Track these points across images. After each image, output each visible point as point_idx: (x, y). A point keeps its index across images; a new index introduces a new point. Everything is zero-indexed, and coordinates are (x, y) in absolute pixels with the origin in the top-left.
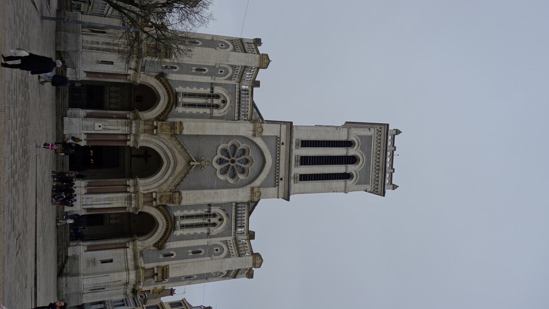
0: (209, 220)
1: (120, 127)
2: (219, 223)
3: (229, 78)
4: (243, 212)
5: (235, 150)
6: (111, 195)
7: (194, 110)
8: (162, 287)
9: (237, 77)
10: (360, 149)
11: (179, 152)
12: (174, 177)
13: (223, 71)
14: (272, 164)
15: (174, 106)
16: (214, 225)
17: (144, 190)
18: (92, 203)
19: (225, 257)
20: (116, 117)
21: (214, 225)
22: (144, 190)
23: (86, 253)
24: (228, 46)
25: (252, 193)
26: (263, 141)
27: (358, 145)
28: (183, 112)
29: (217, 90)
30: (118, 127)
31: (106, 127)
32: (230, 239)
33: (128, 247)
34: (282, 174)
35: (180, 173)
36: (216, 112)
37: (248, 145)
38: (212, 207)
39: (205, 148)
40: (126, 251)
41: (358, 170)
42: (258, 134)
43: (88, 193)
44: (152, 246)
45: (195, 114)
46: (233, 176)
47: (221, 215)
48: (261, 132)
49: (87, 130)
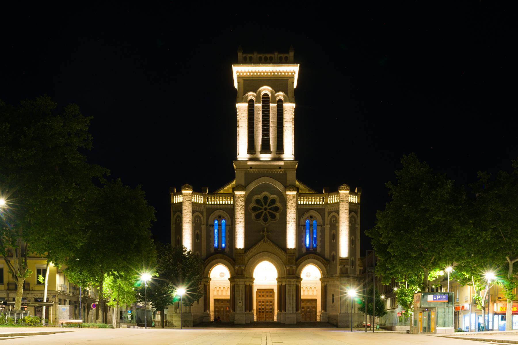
3: (201, 214)
6: (287, 295)
13: (197, 219)
18: (292, 307)
20: (234, 292)
22: (285, 274)
28: (228, 247)
30: (240, 291)
31: (240, 299)
38: (301, 224)
43: (285, 310)
49: (243, 310)
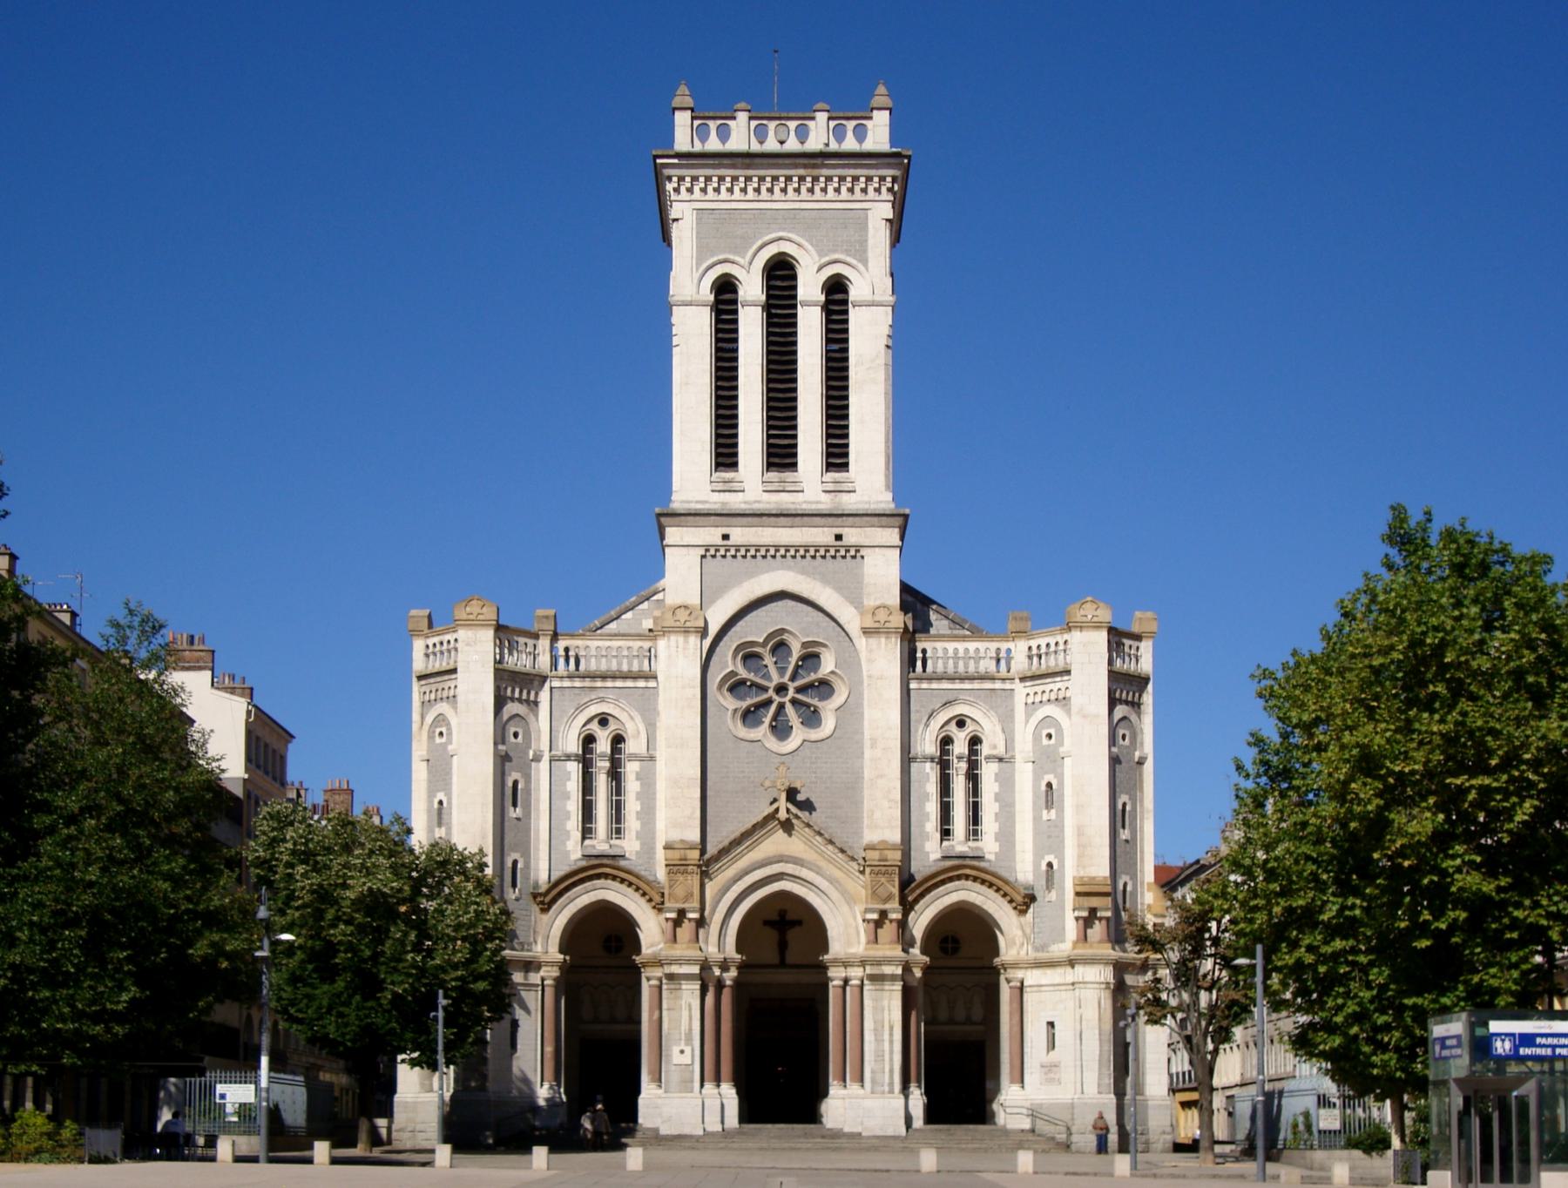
0: (960, 758)
1: (683, 1002)
2: (970, 727)
4: (940, 654)
5: (748, 683)
7: (632, 806)
8: (1148, 890)
10: (743, 258)
11: (750, 849)
12: (823, 864)
14: (789, 568)
15: (622, 863)
16: (975, 741)
17: (859, 943)
18: (887, 1070)
19: (1068, 712)
21: (975, 741)
23: (1026, 1086)
24: (441, 717)
25: (879, 632)
26: (718, 599)
27: (729, 264)
28: (637, 838)
29: (573, 745)
32: (1021, 690)
33: (1022, 983)
34: (821, 535)
35: (812, 846)
36: (633, 746)
37: (730, 646)
39: (741, 775)
40: (1030, 986)
41: (817, 258)
42: (696, 619)
44: (1022, 919)
45: (642, 804)
46: (824, 687)
47: (947, 722)
48: (688, 612)
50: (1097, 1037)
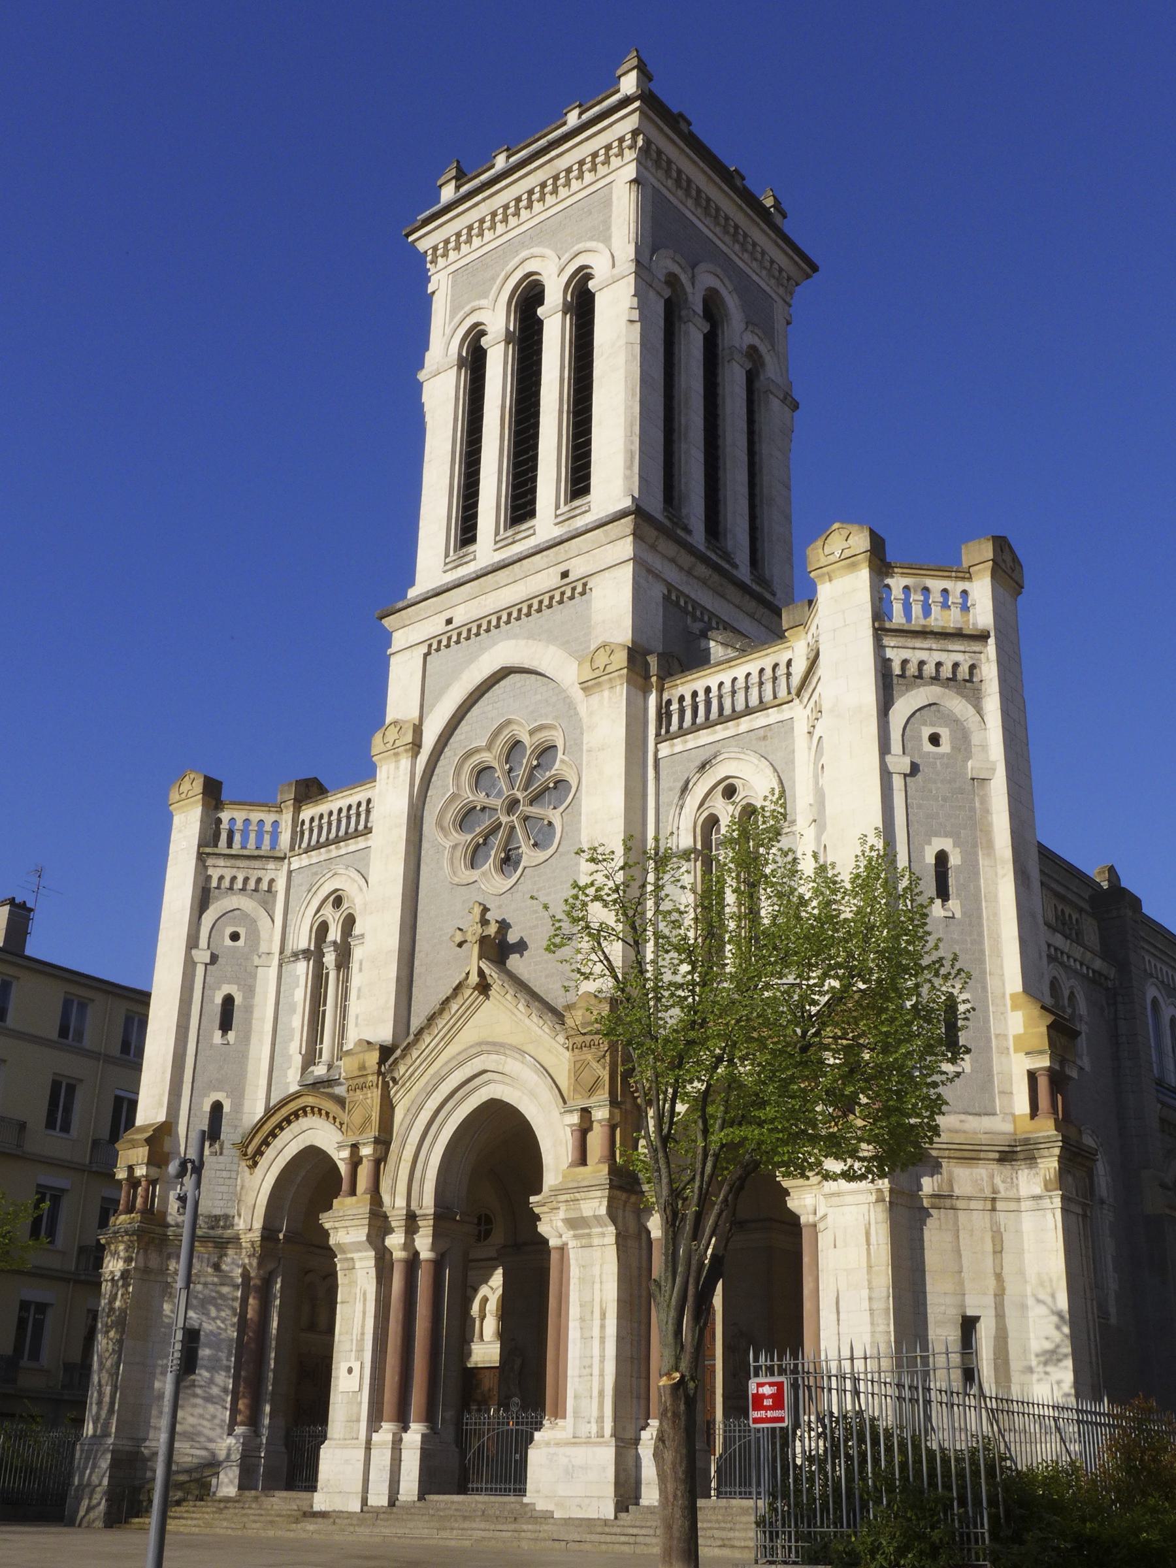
9: (260, 873)
29: (302, 939)
49: (358, 1421)
50: (865, 1305)
